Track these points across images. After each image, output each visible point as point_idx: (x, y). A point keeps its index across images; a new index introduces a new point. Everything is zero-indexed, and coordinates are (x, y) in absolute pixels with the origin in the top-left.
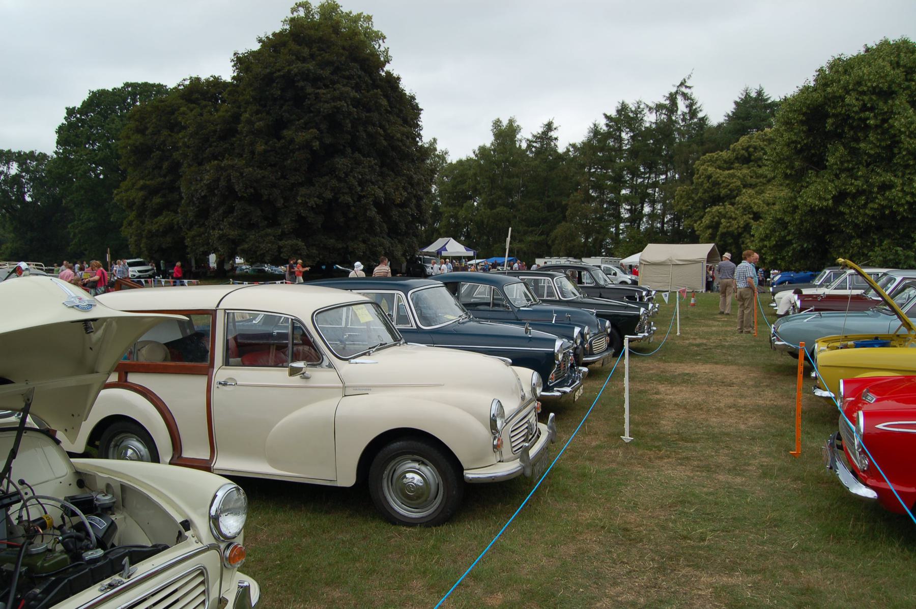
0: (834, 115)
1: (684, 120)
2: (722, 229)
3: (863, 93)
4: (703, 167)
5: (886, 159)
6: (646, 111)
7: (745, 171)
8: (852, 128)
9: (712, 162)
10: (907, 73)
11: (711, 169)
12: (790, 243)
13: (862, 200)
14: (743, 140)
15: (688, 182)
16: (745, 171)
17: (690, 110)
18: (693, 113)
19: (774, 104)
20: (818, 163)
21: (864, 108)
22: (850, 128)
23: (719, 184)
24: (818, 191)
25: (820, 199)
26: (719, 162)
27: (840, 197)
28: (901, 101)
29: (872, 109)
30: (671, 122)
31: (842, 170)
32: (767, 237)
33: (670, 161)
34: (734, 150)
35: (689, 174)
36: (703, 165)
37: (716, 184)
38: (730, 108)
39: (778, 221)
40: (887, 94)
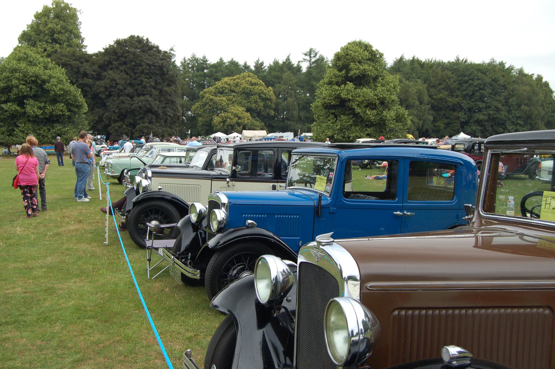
2: (227, 123)
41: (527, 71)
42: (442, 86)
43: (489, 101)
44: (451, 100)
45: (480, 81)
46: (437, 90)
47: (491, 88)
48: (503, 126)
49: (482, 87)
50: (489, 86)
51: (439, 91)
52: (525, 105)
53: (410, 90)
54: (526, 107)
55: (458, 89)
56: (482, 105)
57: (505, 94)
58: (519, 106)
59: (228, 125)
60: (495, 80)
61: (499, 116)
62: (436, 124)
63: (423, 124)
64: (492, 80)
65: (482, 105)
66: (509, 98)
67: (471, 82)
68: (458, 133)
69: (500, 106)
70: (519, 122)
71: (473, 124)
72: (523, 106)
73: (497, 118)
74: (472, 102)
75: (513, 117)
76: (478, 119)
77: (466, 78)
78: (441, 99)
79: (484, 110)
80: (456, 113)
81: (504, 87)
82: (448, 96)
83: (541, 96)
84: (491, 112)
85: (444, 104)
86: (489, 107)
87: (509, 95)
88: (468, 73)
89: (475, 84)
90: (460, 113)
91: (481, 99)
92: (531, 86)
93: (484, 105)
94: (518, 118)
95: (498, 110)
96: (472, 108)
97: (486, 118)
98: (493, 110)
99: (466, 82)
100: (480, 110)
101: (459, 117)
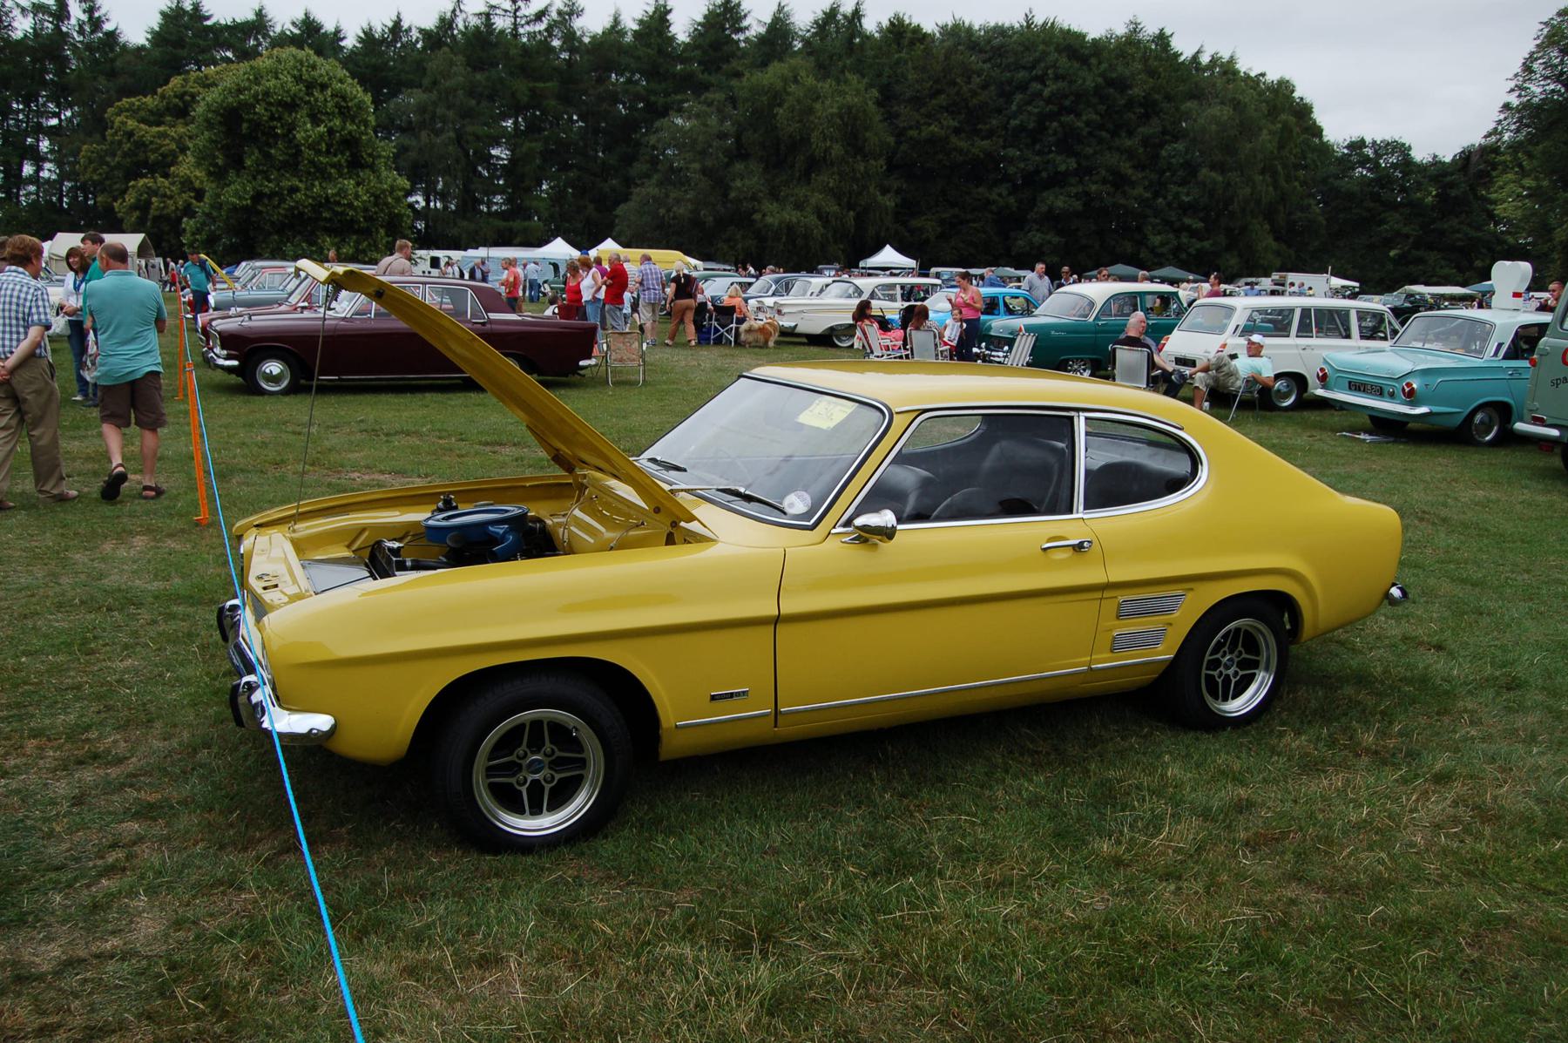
0: (249, 121)
1: (81, 31)
2: (153, 212)
3: (270, 104)
4: (119, 119)
5: (292, 164)
6: (16, 12)
7: (181, 129)
8: (264, 133)
9: (133, 112)
10: (308, 87)
11: (132, 124)
12: (219, 238)
13: (276, 201)
14: (176, 81)
15: (98, 136)
16: (181, 129)
17: (91, 18)
18: (96, 24)
19: (218, 30)
20: (237, 163)
21: (272, 118)
22: (261, 135)
23: (144, 144)
24: (237, 191)
25: (240, 198)
26: (142, 113)
27: (258, 197)
28: (301, 115)
29: (280, 119)
30: (60, 37)
31: (259, 172)
32: (198, 231)
33: (61, 94)
34: (163, 97)
35: (95, 124)
36: (118, 114)
37: (141, 145)
38: (155, 22)
39: (208, 215)
40: (292, 106)
41: (1243, 66)
42: (942, 99)
43: (1090, 151)
44: (963, 144)
45: (1061, 84)
46: (923, 110)
47: (1102, 108)
49: (1067, 103)
50: (1095, 100)
51: (929, 116)
52: (1213, 167)
53: (818, 106)
54: (1213, 174)
55: (999, 111)
56: (1066, 164)
57: (1152, 128)
58: (1191, 168)
59: (156, 219)
60: (1121, 85)
61: (1122, 201)
62: (915, 223)
63: (857, 218)
64: (1111, 83)
65: (1066, 164)
66: (1161, 145)
67: (1036, 86)
68: (878, 248)
69: (1126, 168)
70: (1187, 221)
71: (1036, 227)
72: (1204, 171)
74: (1039, 153)
75: (1169, 205)
76: (1051, 210)
77: (1022, 74)
78: (932, 140)
79: (1073, 180)
80: (980, 190)
81: (1149, 108)
82: (957, 131)
83: (1266, 138)
84: (1094, 188)
85: (940, 156)
87: (1164, 133)
88: (1028, 59)
89: (1046, 93)
90: (996, 190)
91: (1068, 142)
92: (1237, 105)
93: (1072, 163)
94: (1186, 209)
95: (1119, 181)
96: (1037, 172)
97: (1078, 205)
98: (1104, 182)
99: (1023, 87)
100: (1058, 180)
101: (988, 202)
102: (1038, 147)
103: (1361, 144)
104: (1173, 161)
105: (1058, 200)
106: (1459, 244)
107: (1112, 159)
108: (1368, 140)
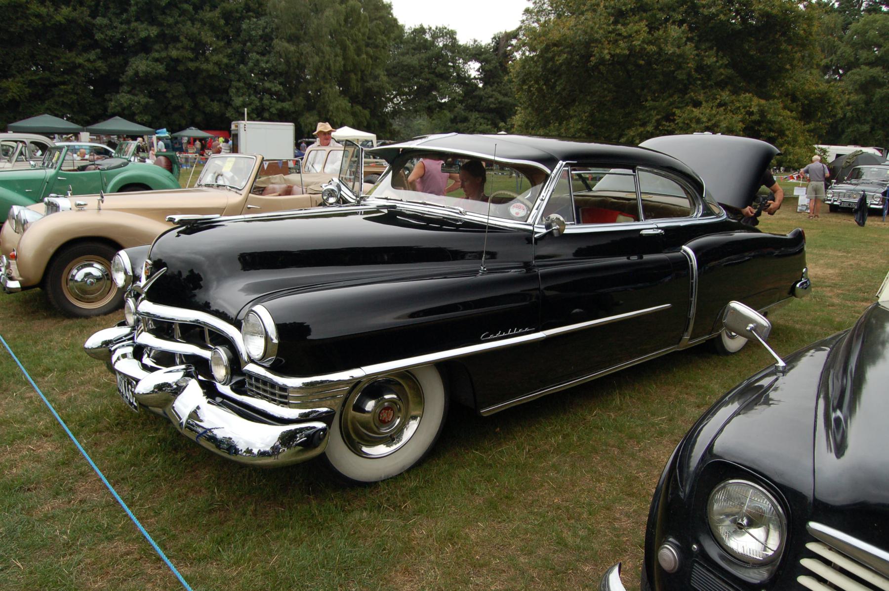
43: (170, 20)
48: (225, 98)
61: (204, 66)
69: (208, 37)
70: (267, 85)
73: (198, 71)
76: (136, 74)
86: (175, 39)
93: (154, 31)
97: (161, 68)
98: (186, 48)
100: (145, 46)
102: (124, 16)
103: (421, 31)
104: (253, 33)
105: (140, 65)
106: (492, 106)
107: (189, 29)
108: (426, 26)
